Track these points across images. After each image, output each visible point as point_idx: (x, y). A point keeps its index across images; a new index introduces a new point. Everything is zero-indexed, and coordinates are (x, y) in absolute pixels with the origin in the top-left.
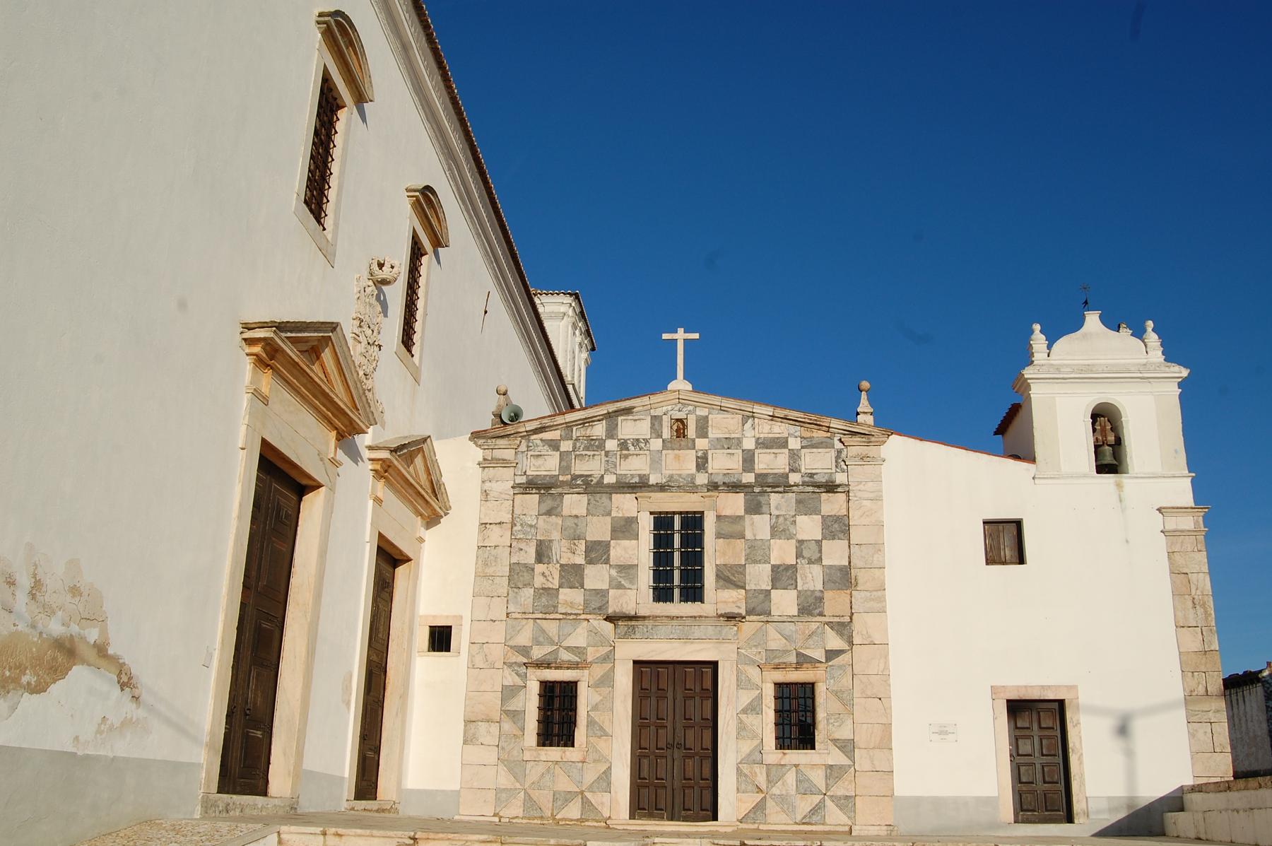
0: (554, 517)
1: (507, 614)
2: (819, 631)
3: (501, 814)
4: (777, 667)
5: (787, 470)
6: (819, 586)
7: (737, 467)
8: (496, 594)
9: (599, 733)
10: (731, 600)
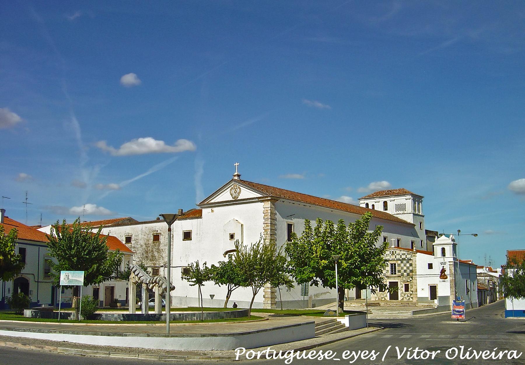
4: (404, 282)
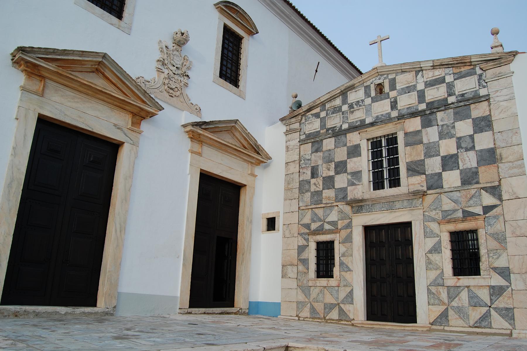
0: (319, 152)
1: (299, 207)
2: (477, 194)
3: (300, 315)
4: (449, 222)
5: (446, 96)
6: (475, 165)
7: (414, 102)
8: (293, 198)
9: (346, 269)
10: (417, 182)
